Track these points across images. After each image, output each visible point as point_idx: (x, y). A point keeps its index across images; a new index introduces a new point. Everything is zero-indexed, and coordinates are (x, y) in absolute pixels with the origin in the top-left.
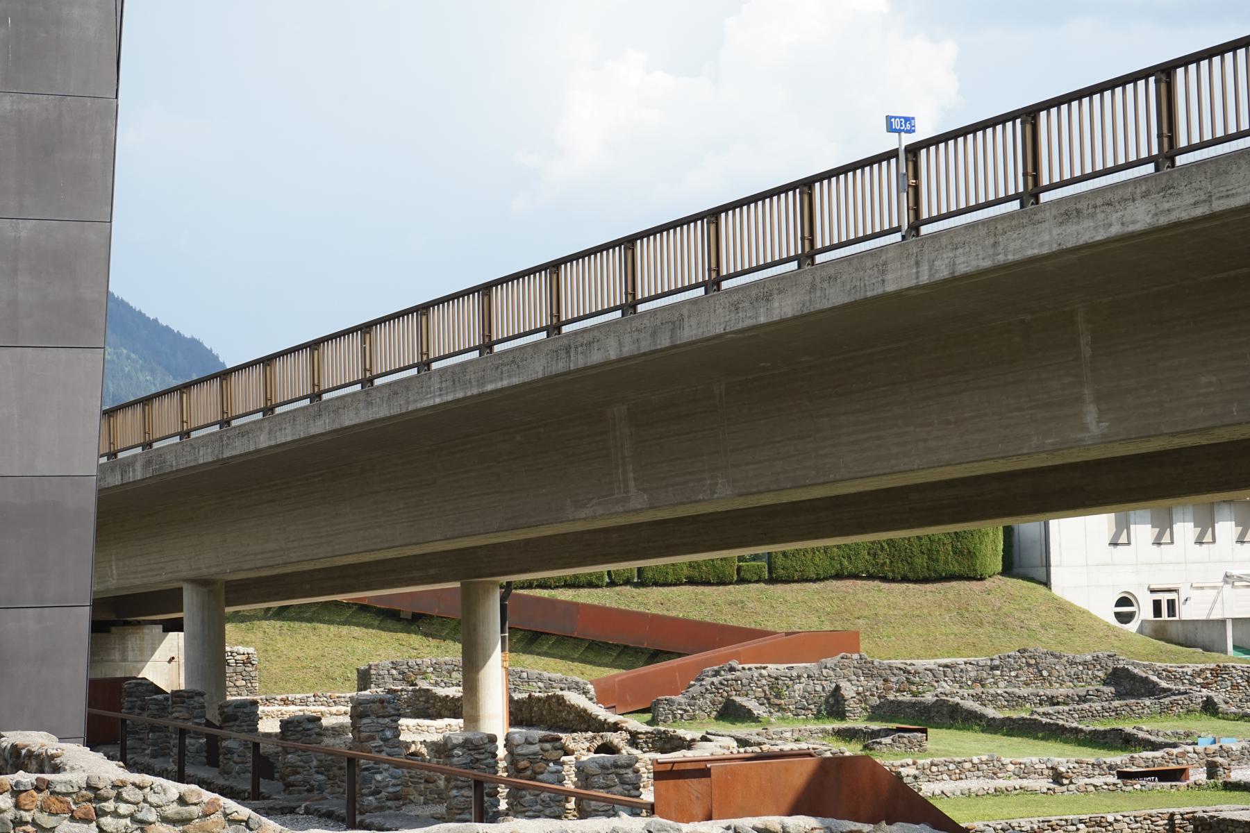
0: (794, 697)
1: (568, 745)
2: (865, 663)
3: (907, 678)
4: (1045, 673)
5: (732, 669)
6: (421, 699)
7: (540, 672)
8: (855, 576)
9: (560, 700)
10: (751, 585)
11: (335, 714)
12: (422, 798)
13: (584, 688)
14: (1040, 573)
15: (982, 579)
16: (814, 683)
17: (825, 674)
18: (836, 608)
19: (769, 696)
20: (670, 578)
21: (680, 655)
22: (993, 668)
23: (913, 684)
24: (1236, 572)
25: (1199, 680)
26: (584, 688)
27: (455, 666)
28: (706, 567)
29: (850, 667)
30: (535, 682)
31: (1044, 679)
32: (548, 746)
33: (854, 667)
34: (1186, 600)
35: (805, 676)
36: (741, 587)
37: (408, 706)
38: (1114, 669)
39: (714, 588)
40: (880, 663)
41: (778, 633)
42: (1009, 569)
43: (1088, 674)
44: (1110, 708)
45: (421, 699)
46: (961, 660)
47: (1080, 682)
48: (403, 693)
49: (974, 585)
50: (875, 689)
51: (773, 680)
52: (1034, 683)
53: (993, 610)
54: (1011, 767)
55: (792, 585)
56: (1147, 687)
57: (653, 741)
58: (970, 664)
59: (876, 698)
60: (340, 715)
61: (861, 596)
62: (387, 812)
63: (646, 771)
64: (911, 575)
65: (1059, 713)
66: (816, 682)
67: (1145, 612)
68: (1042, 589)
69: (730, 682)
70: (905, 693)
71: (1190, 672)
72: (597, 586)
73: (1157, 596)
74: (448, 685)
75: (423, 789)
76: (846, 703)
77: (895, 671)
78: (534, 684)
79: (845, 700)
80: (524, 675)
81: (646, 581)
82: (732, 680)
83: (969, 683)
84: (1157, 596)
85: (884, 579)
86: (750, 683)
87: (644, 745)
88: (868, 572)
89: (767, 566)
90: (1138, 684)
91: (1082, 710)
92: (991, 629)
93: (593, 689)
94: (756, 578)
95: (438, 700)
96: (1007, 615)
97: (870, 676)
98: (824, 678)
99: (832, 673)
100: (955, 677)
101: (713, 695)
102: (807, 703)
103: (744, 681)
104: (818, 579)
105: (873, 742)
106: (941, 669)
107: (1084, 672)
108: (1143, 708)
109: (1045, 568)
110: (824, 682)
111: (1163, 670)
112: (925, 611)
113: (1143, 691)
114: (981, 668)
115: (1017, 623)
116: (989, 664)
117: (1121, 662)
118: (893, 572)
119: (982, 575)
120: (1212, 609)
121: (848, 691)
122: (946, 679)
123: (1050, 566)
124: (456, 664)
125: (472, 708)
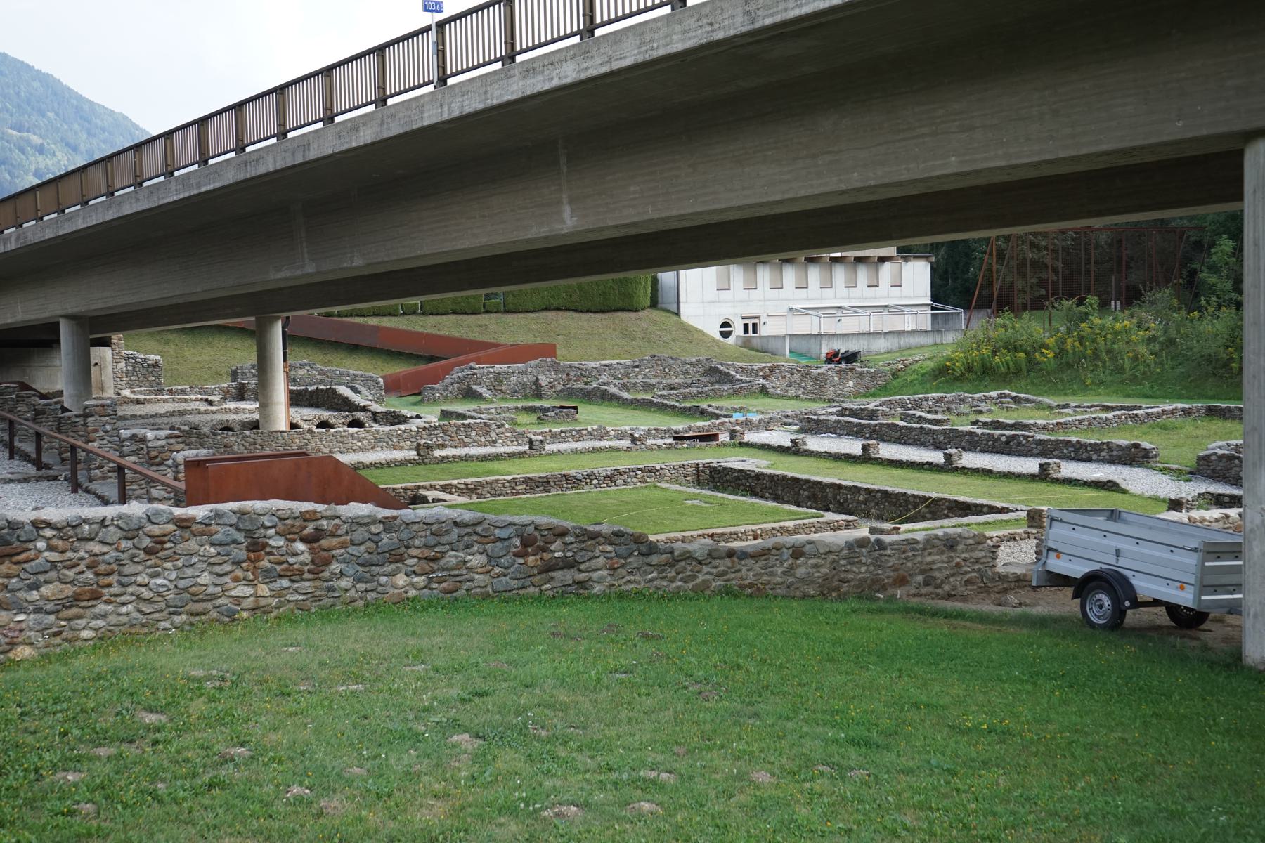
4: (667, 370)
5: (471, 368)
8: (558, 309)
9: (334, 391)
15: (637, 311)
21: (445, 359)
24: (795, 307)
32: (172, 441)
36: (486, 316)
42: (654, 304)
49: (632, 315)
54: (612, 433)
61: (561, 322)
62: (109, 480)
64: (593, 309)
67: (738, 330)
68: (675, 318)
71: (755, 368)
72: (394, 315)
73: (746, 321)
84: (746, 321)
85: (576, 311)
121: (544, 380)
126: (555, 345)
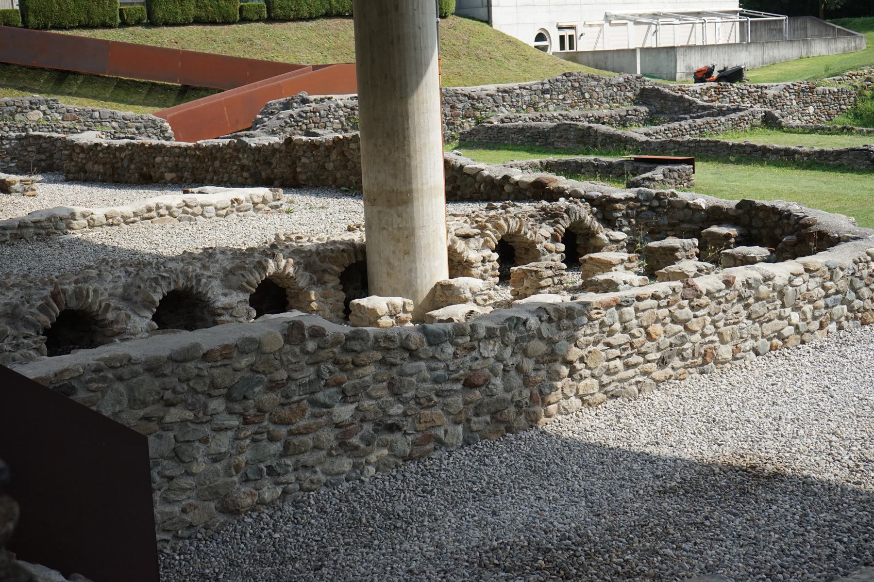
1: (526, 234)
3: (472, 104)
4: (587, 96)
5: (304, 101)
6: (29, 149)
7: (113, 111)
10: (253, 24)
12: (460, 428)
13: (161, 127)
14: (483, 12)
18: (334, 44)
20: (179, 18)
21: (209, 91)
22: (544, 92)
23: (478, 109)
25: (706, 98)
26: (161, 127)
27: (18, 107)
28: (212, 7)
30: (109, 122)
31: (586, 101)
34: (582, 35)
36: (245, 26)
37: (13, 159)
38: (641, 89)
39: (220, 27)
40: (447, 90)
41: (306, 66)
43: (621, 96)
44: (695, 126)
45: (29, 149)
46: (515, 85)
47: (614, 103)
51: (349, 110)
52: (578, 106)
53: (464, 44)
55: (289, 23)
56: (682, 105)
57: (638, 213)
58: (525, 88)
63: (824, 293)
65: (657, 133)
69: (308, 114)
70: (470, 119)
72: (110, 27)
73: (562, 33)
74: (12, 129)
75: (462, 406)
77: (461, 98)
78: (108, 123)
80: (96, 114)
82: (311, 112)
83: (524, 107)
84: (562, 33)
86: (328, 114)
87: (625, 222)
89: (265, 6)
90: (670, 103)
91: (675, 129)
92: (467, 59)
93: (170, 127)
94: (256, 17)
95: (77, 151)
96: (477, 48)
100: (512, 102)
101: (292, 128)
103: (322, 112)
105: (644, 179)
106: (500, 94)
107: (618, 93)
108: (719, 125)
109: (486, 8)
111: (679, 89)
113: (676, 109)
114: (533, 92)
115: (486, 54)
116: (540, 88)
117: (646, 83)
119: (446, 13)
120: (597, 43)
122: (505, 103)
123: (491, 6)
124: (19, 104)
125: (395, 176)
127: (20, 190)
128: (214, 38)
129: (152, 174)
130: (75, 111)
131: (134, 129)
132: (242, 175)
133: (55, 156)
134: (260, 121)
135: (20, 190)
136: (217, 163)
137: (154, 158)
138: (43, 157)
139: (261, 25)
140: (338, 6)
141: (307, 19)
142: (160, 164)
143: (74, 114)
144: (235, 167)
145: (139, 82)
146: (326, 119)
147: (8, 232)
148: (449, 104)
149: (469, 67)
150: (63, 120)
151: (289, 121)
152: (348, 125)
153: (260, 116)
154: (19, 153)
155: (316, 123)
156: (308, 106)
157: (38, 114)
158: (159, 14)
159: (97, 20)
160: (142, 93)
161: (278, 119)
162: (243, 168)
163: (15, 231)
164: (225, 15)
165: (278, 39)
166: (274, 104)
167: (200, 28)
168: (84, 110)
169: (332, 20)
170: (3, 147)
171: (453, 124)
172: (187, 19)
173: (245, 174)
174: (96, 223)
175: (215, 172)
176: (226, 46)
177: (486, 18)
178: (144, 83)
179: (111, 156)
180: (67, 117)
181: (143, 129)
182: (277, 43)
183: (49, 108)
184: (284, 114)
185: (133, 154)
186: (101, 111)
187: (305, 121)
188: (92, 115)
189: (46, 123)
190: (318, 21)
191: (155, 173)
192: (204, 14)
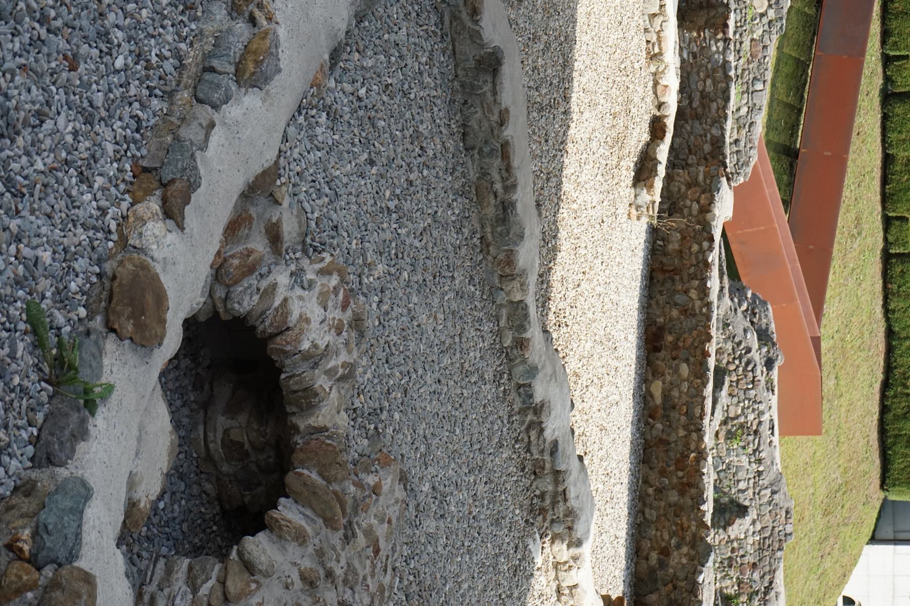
0: (728, 455)
2: (780, 540)
3: (758, 591)
5: (769, 364)
8: (890, 350)
10: (881, 234)
11: (656, 84)
13: (738, 174)
14: (887, 531)
16: (749, 479)
17: (763, 492)
18: (849, 346)
19: (730, 424)
20: (893, 136)
23: (750, 599)
26: (738, 174)
29: (773, 522)
30: (747, 103)
33: (774, 527)
35: (761, 469)
37: (695, 57)
39: (878, 189)
40: (780, 558)
45: (709, 82)
48: (721, 44)
49: (878, 482)
50: (741, 552)
55: (881, 282)
59: (729, 554)
60: (655, 93)
64: (889, 416)
66: (752, 481)
72: (883, 42)
76: (721, 531)
77: (767, 578)
78: (746, 101)
79: (725, 529)
80: (759, 86)
81: (891, 105)
82: (754, 377)
85: (886, 385)
86: (749, 400)
88: (896, 368)
89: (906, 251)
92: (821, 526)
94: (891, 239)
96: (837, 537)
97: (761, 548)
98: (757, 491)
99: (766, 499)
101: (730, 351)
102: (721, 471)
103: (753, 392)
104: (887, 310)
109: (892, 537)
110: (751, 491)
112: (844, 447)
115: (828, 550)
118: (895, 396)
119: (887, 490)
123: (895, 544)
126: (820, 433)
127: (640, 201)
128: (863, 184)
129: (662, 354)
130: (765, 57)
131: (736, 137)
132: (652, 549)
133: (697, 124)
134: (742, 298)
135: (640, 201)
136: (673, 497)
137: (687, 361)
138: (696, 104)
139: (880, 244)
140: (903, 348)
141: (885, 305)
142: (676, 371)
143: (760, 55)
144: (666, 537)
145: (803, 92)
146: (742, 397)
147: (547, 457)
148: (759, 560)
149: (811, 531)
150: (752, 40)
151: (742, 347)
152: (733, 426)
153: (749, 295)
154: (702, 65)
155: (737, 384)
156: (762, 372)
157: (762, 7)
158: (899, 109)
159: (893, 24)
160: (788, 96)
161: (745, 331)
162: (665, 552)
163: (548, 466)
164: (895, 198)
165: (858, 271)
166: (766, 316)
167: (879, 163)
168: (766, 69)
169: (884, 340)
170: (712, 42)
171: (730, 566)
172: (891, 145)
173: (654, 556)
174: (563, 573)
175: (659, 491)
176: (852, 202)
177: (878, 536)
178: (802, 97)
179: (692, 270)
180: (756, 46)
181: (736, 149)
182: (853, 270)
183: (770, 22)
184: (752, 339)
185: (694, 315)
186: (764, 92)
187: (741, 369)
188: (759, 80)
189: (749, 18)
190: (883, 320)
191: (663, 360)
192: (898, 168)
